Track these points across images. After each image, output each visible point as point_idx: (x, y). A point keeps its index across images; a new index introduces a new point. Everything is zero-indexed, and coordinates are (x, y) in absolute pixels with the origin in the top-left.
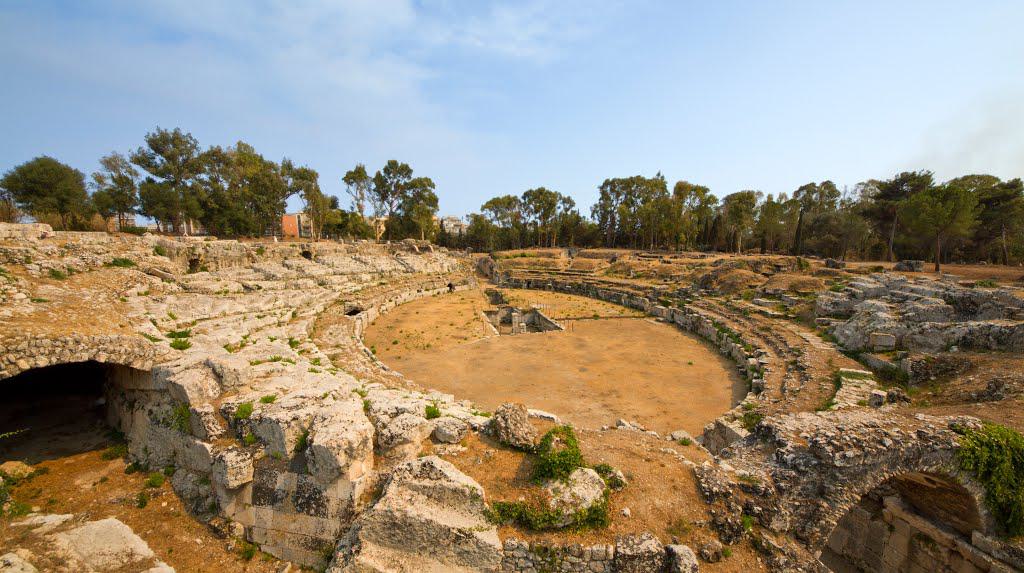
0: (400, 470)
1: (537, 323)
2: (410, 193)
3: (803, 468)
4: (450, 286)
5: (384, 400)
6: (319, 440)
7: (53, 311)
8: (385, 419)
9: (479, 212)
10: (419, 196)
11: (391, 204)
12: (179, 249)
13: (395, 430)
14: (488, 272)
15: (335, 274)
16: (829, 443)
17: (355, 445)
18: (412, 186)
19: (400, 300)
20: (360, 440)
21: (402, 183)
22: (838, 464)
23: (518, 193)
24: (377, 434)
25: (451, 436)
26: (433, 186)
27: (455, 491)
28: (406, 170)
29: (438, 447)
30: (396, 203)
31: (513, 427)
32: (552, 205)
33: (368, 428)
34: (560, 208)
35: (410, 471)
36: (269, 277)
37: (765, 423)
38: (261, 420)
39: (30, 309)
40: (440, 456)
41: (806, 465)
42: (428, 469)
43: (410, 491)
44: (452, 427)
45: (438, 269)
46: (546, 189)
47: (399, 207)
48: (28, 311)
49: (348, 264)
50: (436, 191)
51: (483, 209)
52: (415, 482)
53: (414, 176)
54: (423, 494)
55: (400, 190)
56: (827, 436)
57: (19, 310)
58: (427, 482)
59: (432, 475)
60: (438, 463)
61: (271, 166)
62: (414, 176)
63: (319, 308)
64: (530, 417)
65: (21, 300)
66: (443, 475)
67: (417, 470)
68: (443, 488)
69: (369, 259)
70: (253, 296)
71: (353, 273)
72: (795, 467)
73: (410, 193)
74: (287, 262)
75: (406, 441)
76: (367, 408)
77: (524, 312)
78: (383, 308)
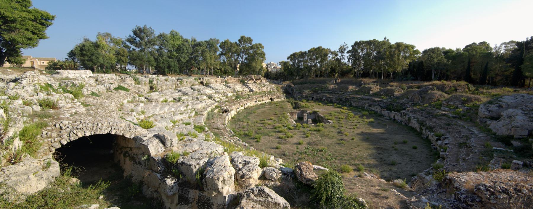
0: (248, 192)
1: (317, 119)
2: (251, 52)
3: (470, 203)
4: (271, 99)
5: (240, 156)
6: (209, 175)
7: (92, 110)
8: (241, 166)
9: (286, 60)
10: (255, 53)
11: (242, 58)
12: (145, 81)
13: (244, 171)
14: (291, 92)
15: (216, 93)
16: (487, 190)
17: (226, 179)
18: (252, 47)
19: (246, 106)
20: (229, 176)
21: (247, 46)
22: (492, 201)
23: (306, 49)
24: (236, 174)
25: (272, 176)
26: (263, 47)
27: (275, 204)
28: (250, 40)
29: (267, 182)
30: (244, 57)
31: (305, 174)
32: (326, 55)
33: (233, 171)
34: (330, 57)
35: (253, 193)
36: (186, 94)
37: (448, 177)
38: (183, 163)
39: (83, 109)
40: (267, 186)
41: (473, 201)
42: (261, 192)
43: (253, 203)
44: (274, 172)
45: (265, 90)
46: (323, 47)
47: (246, 59)
48: (82, 110)
49: (221, 87)
50: (265, 50)
51: (288, 58)
52: (255, 198)
53: (253, 43)
54: (259, 204)
55: (246, 51)
56: (486, 186)
57: (78, 110)
58: (261, 199)
59: (264, 195)
60: (267, 190)
61: (187, 41)
62: (253, 43)
63: (209, 109)
64: (314, 169)
65: (79, 105)
66: (268, 196)
67: (256, 192)
68: (269, 203)
69: (231, 85)
70: (179, 104)
71: (224, 93)
72: (465, 202)
73: (251, 52)
74: (193, 87)
75: (250, 177)
76: (232, 161)
77: (310, 113)
78: (238, 110)
